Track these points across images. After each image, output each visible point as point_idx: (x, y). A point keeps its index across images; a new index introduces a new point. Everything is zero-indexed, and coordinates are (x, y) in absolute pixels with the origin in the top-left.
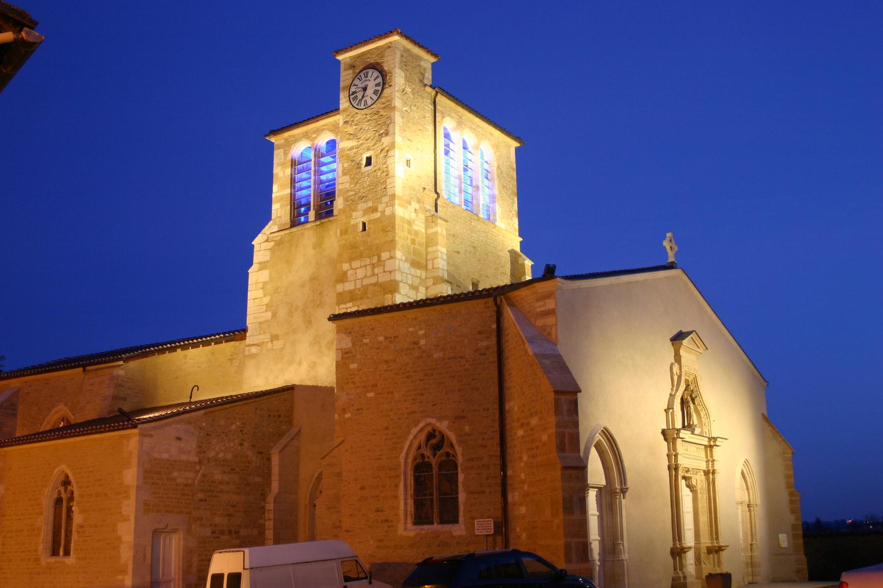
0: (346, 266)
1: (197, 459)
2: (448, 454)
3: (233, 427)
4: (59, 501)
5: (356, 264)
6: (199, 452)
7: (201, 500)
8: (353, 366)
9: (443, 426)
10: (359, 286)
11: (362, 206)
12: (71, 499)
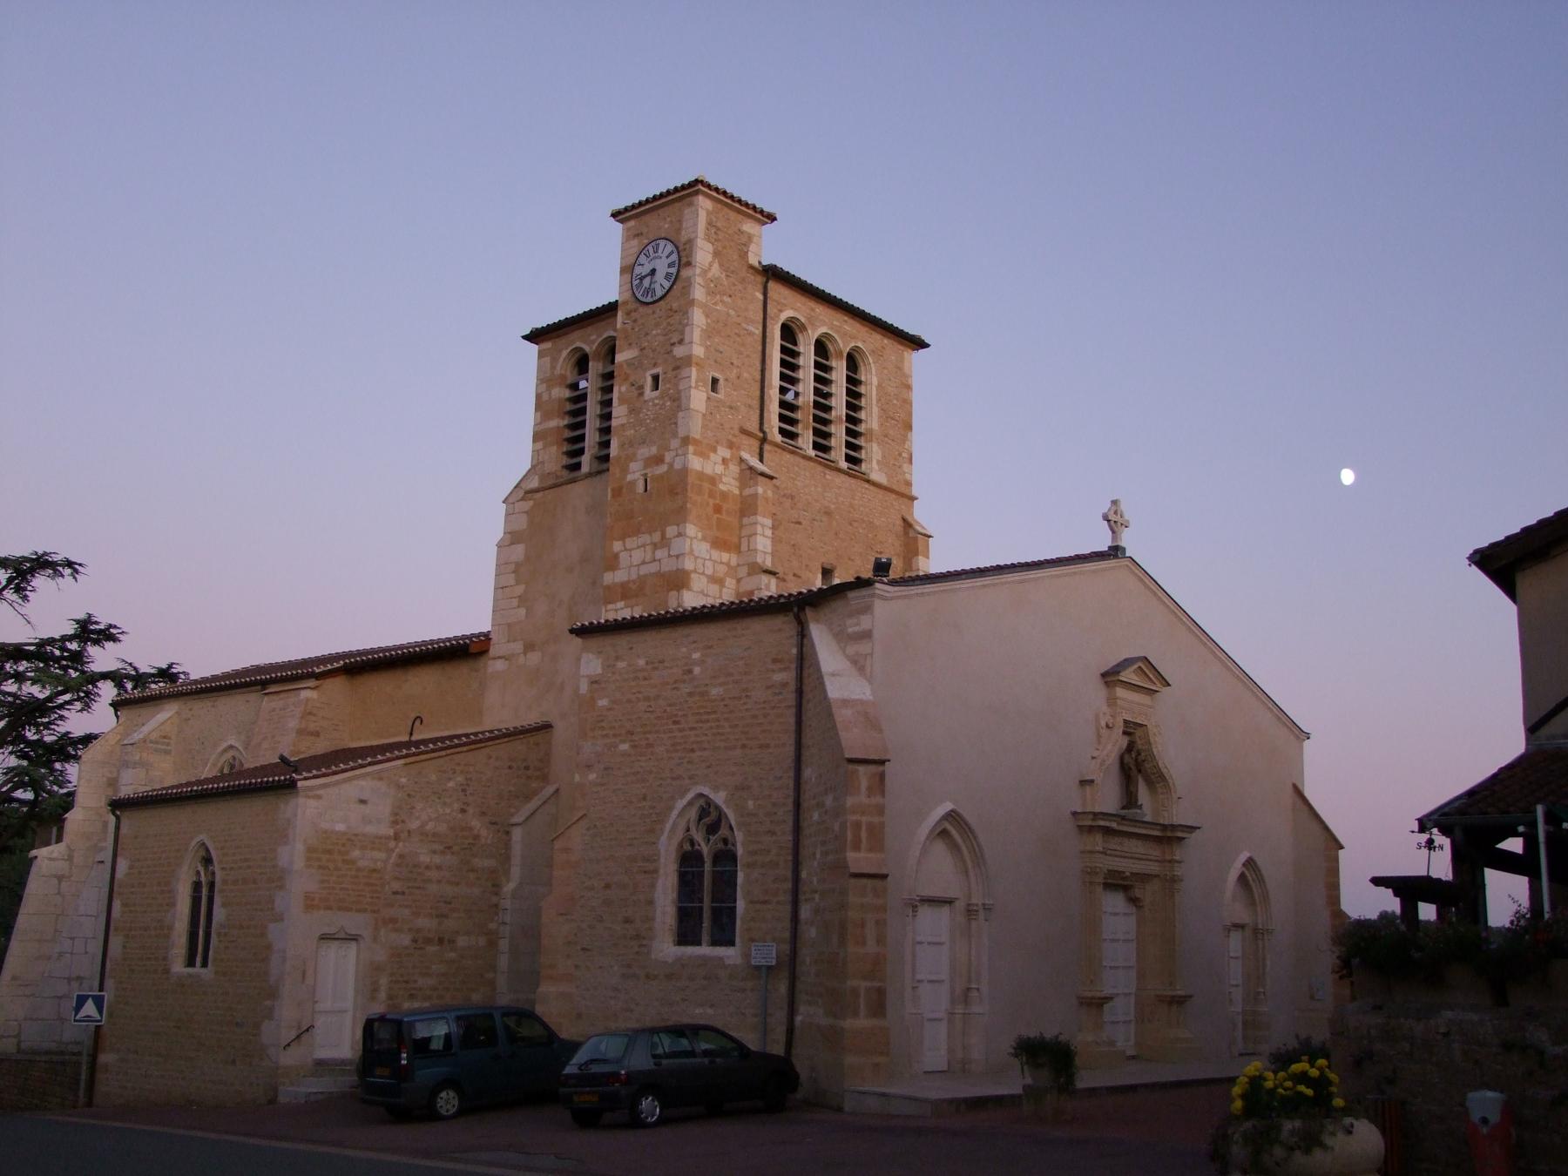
0: (617, 546)
1: (391, 832)
2: (725, 841)
3: (451, 784)
4: (197, 886)
5: (630, 543)
6: (395, 822)
7: (395, 893)
8: (603, 702)
9: (719, 798)
10: (634, 576)
11: (645, 452)
12: (212, 885)
